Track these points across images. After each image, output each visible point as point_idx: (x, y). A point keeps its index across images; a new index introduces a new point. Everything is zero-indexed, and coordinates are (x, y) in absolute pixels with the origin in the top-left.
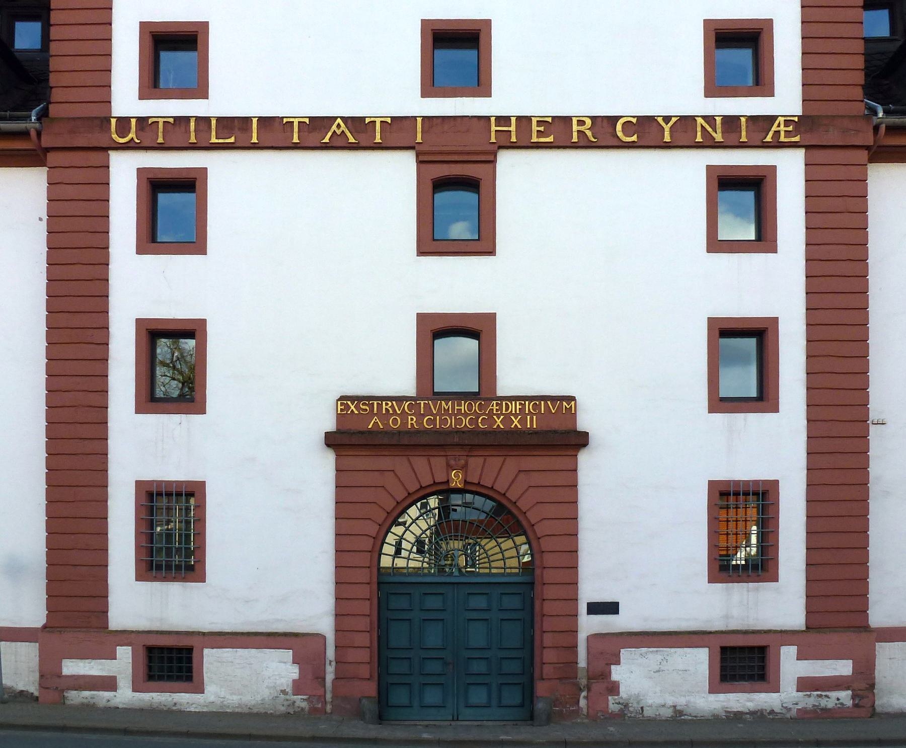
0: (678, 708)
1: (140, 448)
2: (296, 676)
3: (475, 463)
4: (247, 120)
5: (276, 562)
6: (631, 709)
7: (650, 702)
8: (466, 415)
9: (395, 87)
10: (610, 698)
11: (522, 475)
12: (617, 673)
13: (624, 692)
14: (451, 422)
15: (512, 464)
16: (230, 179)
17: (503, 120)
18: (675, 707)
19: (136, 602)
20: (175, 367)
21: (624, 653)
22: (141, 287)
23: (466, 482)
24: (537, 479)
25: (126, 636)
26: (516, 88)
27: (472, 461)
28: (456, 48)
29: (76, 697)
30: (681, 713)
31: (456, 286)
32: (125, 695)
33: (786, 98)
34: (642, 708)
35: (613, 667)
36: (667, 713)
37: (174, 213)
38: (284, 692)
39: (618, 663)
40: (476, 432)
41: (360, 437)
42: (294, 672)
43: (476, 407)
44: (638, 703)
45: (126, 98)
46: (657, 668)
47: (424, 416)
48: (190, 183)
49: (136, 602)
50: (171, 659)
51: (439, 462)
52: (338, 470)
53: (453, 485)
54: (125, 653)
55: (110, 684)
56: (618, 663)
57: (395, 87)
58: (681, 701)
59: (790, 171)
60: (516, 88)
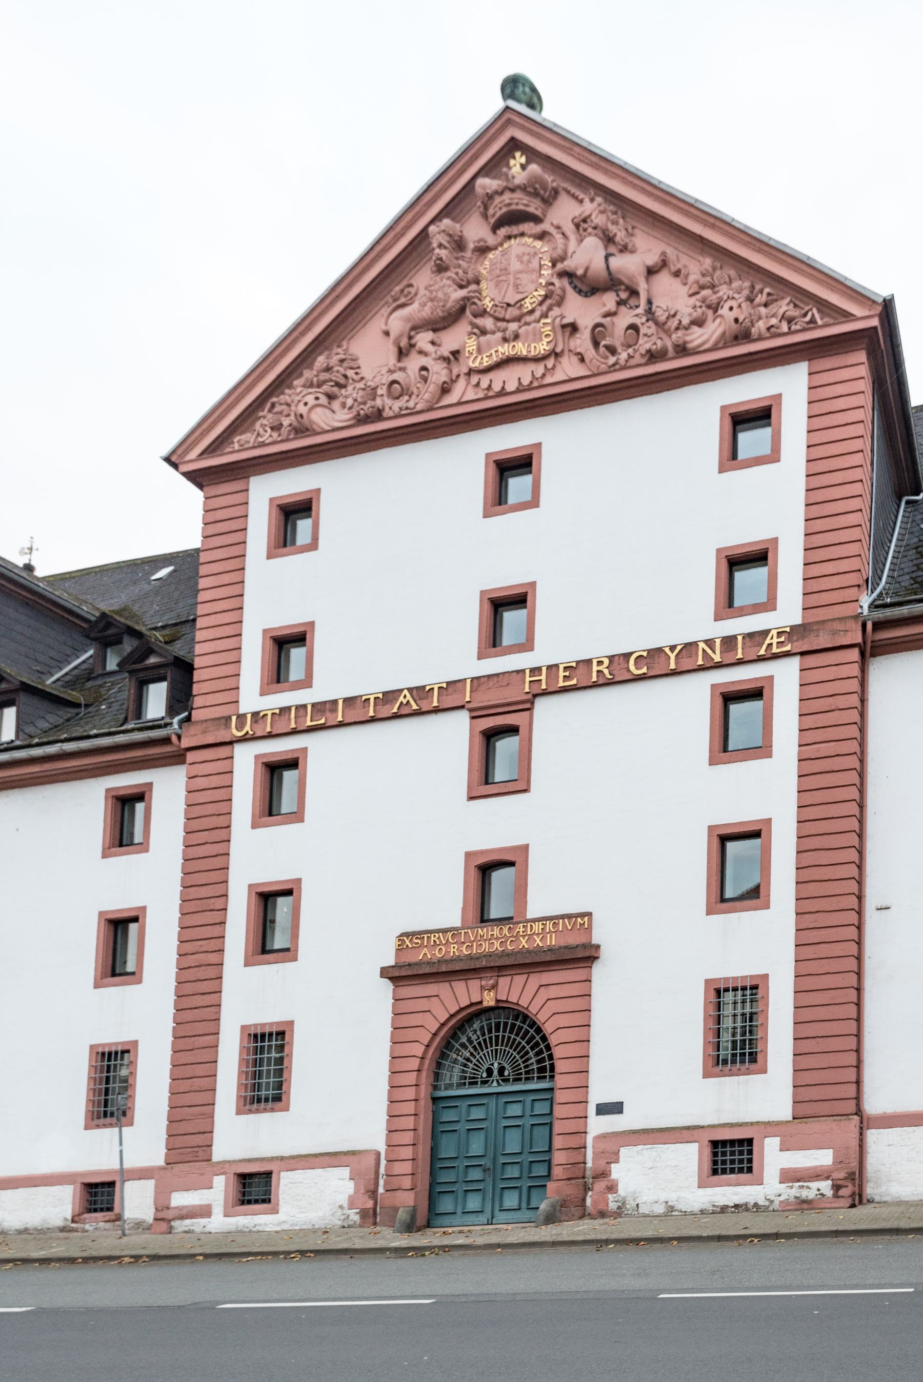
0: (670, 1204)
2: (351, 1191)
3: (504, 982)
6: (628, 1206)
7: (644, 1199)
8: (498, 939)
10: (610, 1196)
11: (542, 988)
12: (616, 1172)
13: (622, 1191)
14: (485, 947)
15: (536, 980)
18: (667, 1202)
21: (623, 1151)
23: (498, 1001)
24: (554, 992)
27: (501, 980)
30: (672, 1209)
34: (637, 1205)
35: (613, 1165)
36: (660, 1209)
38: (341, 1207)
39: (617, 1161)
40: (505, 954)
42: (349, 1187)
43: (505, 931)
44: (634, 1200)
46: (652, 1165)
47: (464, 943)
51: (475, 984)
53: (485, 1004)
56: (617, 1161)
58: (672, 1198)
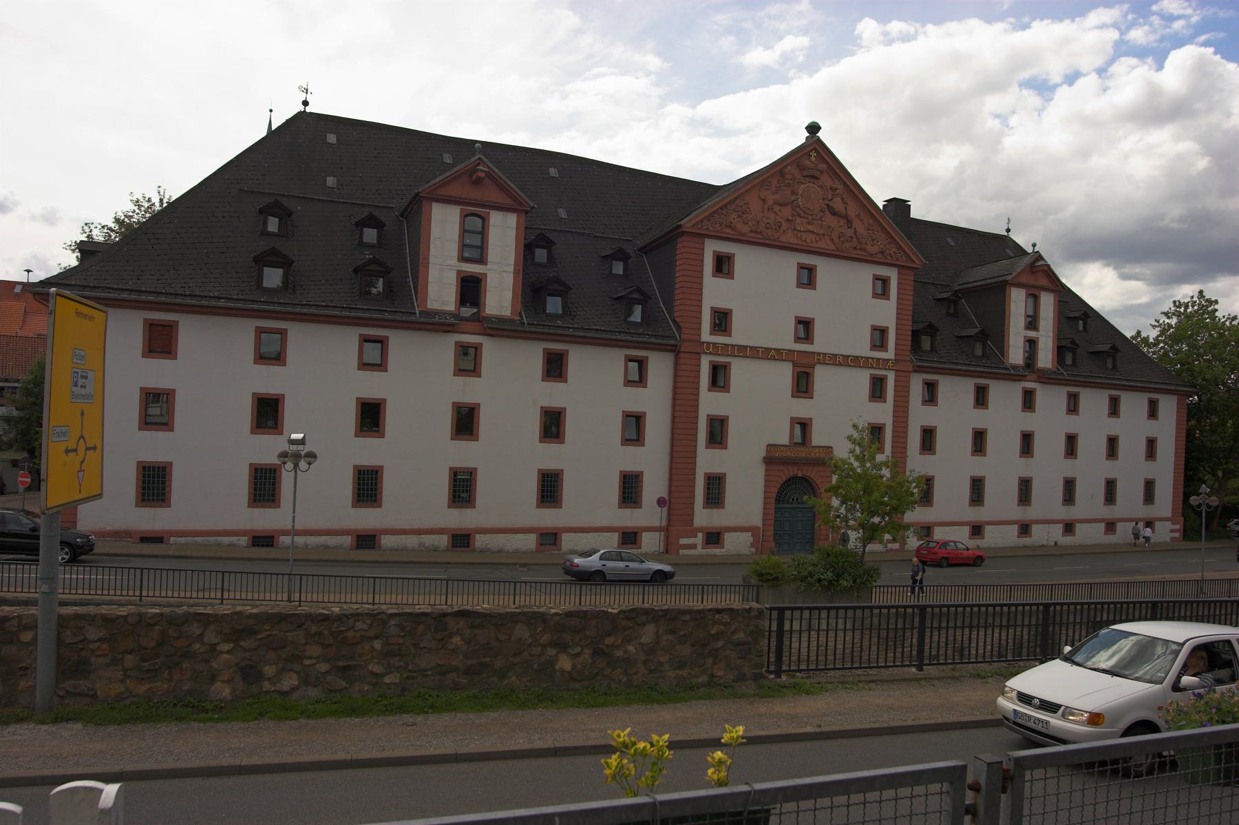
1: (707, 460)
4: (746, 347)
5: (747, 501)
9: (785, 338)
16: (740, 370)
17: (819, 354)
19: (703, 517)
20: (718, 432)
22: (710, 403)
25: (700, 530)
26: (821, 343)
28: (805, 326)
29: (682, 552)
31: (802, 408)
32: (699, 550)
33: (890, 354)
37: (719, 378)
41: (772, 459)
45: (706, 336)
48: (726, 367)
49: (703, 517)
50: (714, 537)
52: (766, 470)
54: (700, 535)
55: (694, 546)
57: (785, 338)
59: (891, 378)
60: (821, 343)
